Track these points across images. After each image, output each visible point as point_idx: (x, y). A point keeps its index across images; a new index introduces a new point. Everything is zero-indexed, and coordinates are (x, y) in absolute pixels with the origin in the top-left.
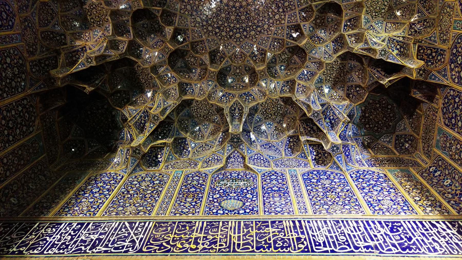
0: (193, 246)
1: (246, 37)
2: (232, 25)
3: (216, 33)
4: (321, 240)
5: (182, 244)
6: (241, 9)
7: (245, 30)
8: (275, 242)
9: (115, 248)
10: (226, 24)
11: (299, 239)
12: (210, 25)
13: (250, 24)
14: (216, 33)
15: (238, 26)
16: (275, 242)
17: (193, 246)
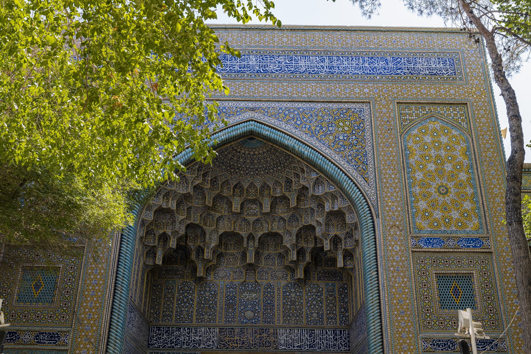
0: (236, 345)
1: (257, 174)
2: (248, 166)
3: (237, 173)
4: (282, 342)
5: (232, 344)
6: (255, 156)
7: (257, 170)
8: (266, 343)
9: (208, 346)
10: (243, 166)
11: (274, 341)
12: (232, 168)
13: (261, 166)
14: (237, 173)
15: (252, 167)
16: (266, 343)
17: (236, 345)
